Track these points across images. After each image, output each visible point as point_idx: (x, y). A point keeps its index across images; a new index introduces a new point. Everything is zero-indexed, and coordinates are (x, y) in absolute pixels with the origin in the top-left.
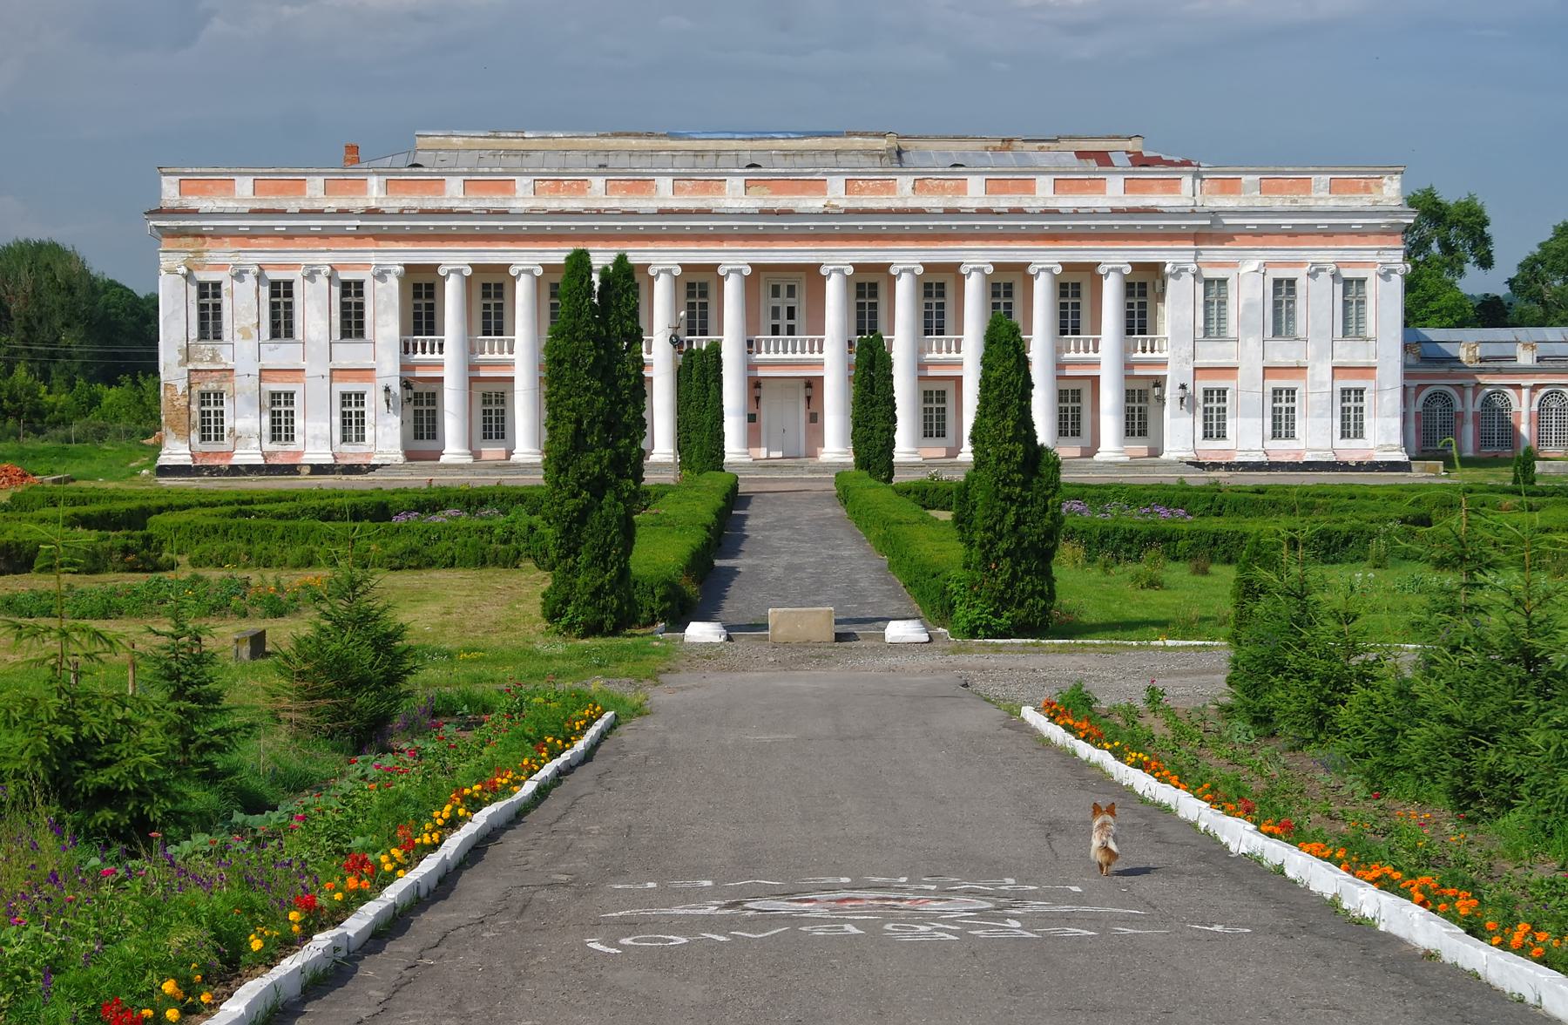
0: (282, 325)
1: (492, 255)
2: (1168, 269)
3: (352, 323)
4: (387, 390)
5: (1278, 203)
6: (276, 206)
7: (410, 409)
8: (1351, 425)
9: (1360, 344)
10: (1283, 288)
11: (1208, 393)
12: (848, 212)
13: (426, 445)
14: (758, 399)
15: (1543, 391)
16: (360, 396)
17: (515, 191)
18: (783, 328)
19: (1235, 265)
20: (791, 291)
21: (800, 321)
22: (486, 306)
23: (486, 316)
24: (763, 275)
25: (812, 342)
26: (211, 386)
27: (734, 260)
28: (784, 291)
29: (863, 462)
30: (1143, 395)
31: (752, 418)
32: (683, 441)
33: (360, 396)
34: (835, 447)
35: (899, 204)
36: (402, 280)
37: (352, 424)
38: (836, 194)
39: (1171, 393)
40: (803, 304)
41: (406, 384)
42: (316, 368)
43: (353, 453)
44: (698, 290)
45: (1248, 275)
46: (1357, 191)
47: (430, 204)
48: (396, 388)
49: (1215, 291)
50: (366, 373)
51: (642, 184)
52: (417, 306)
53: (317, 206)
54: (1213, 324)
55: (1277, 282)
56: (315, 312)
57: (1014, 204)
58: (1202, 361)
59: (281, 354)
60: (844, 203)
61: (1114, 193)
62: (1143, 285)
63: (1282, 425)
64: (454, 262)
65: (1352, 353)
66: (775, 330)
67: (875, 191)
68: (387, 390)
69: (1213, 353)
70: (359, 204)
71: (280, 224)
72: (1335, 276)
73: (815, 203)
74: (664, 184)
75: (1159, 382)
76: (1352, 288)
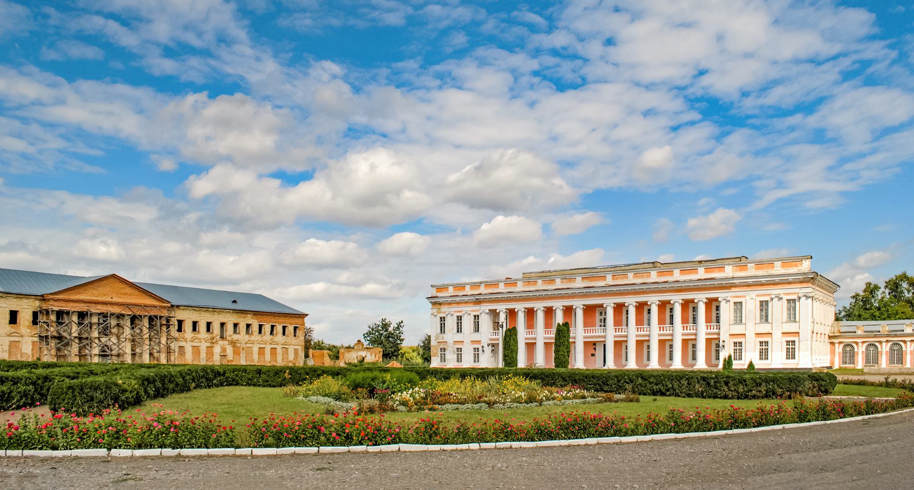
0: (459, 330)
2: (720, 299)
3: (477, 329)
5: (761, 273)
9: (793, 324)
10: (764, 305)
26: (442, 346)
27: (578, 304)
32: (505, 360)
37: (476, 358)
38: (609, 280)
43: (476, 365)
45: (751, 300)
48: (485, 346)
49: (738, 305)
50: (479, 342)
54: (739, 320)
55: (761, 302)
56: (468, 323)
59: (459, 337)
60: (611, 284)
69: (738, 329)
71: (458, 299)
73: (602, 283)
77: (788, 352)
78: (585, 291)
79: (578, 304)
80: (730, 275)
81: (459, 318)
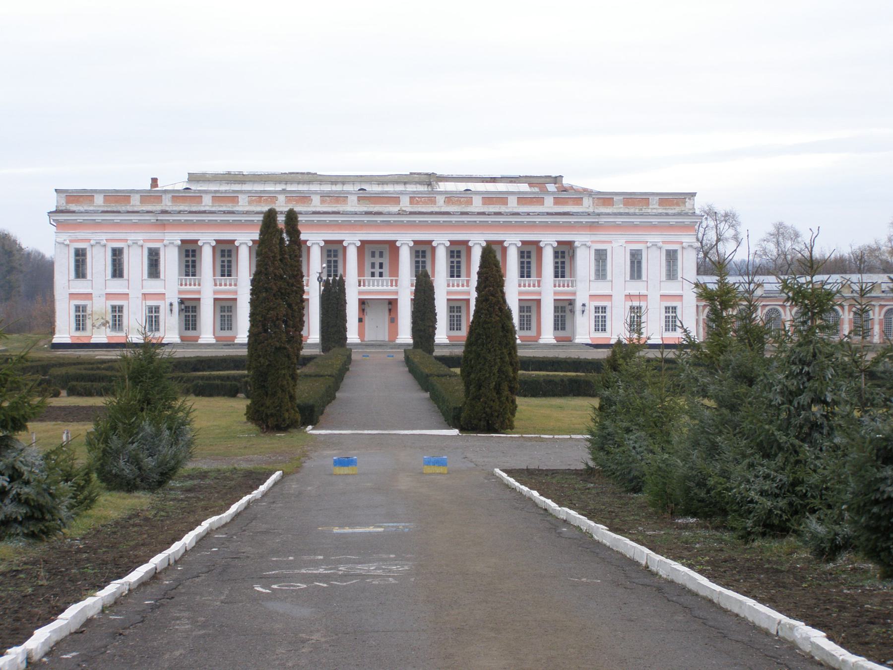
0: (117, 272)
1: (226, 235)
2: (576, 244)
3: (154, 269)
4: (171, 305)
6: (115, 209)
7: (183, 314)
11: (597, 308)
12: (411, 213)
13: (191, 333)
14: (363, 310)
15: (767, 308)
16: (157, 309)
17: (238, 202)
18: (377, 274)
19: (610, 242)
20: (381, 255)
21: (386, 270)
22: (223, 262)
23: (223, 266)
24: (366, 246)
25: (392, 281)
27: (352, 239)
28: (377, 254)
29: (416, 344)
30: (563, 309)
31: (360, 320)
33: (157, 309)
34: (405, 336)
35: (437, 210)
36: (180, 248)
39: (578, 307)
40: (388, 260)
41: (182, 301)
42: (135, 294)
44: (333, 252)
46: (673, 205)
47: (194, 209)
49: (601, 257)
52: (187, 261)
53: (136, 209)
54: (601, 273)
56: (135, 263)
57: (497, 210)
58: (593, 292)
59: (116, 286)
60: (409, 209)
61: (549, 204)
62: (563, 252)
64: (207, 239)
65: (672, 288)
66: (373, 275)
67: (425, 203)
68: (171, 305)
69: (601, 288)
70: (158, 208)
73: (395, 209)
74: (316, 199)
75: (571, 303)
76: (671, 257)
77: (667, 322)
78: (366, 219)
79: (352, 239)
80: (591, 210)
81: (117, 253)
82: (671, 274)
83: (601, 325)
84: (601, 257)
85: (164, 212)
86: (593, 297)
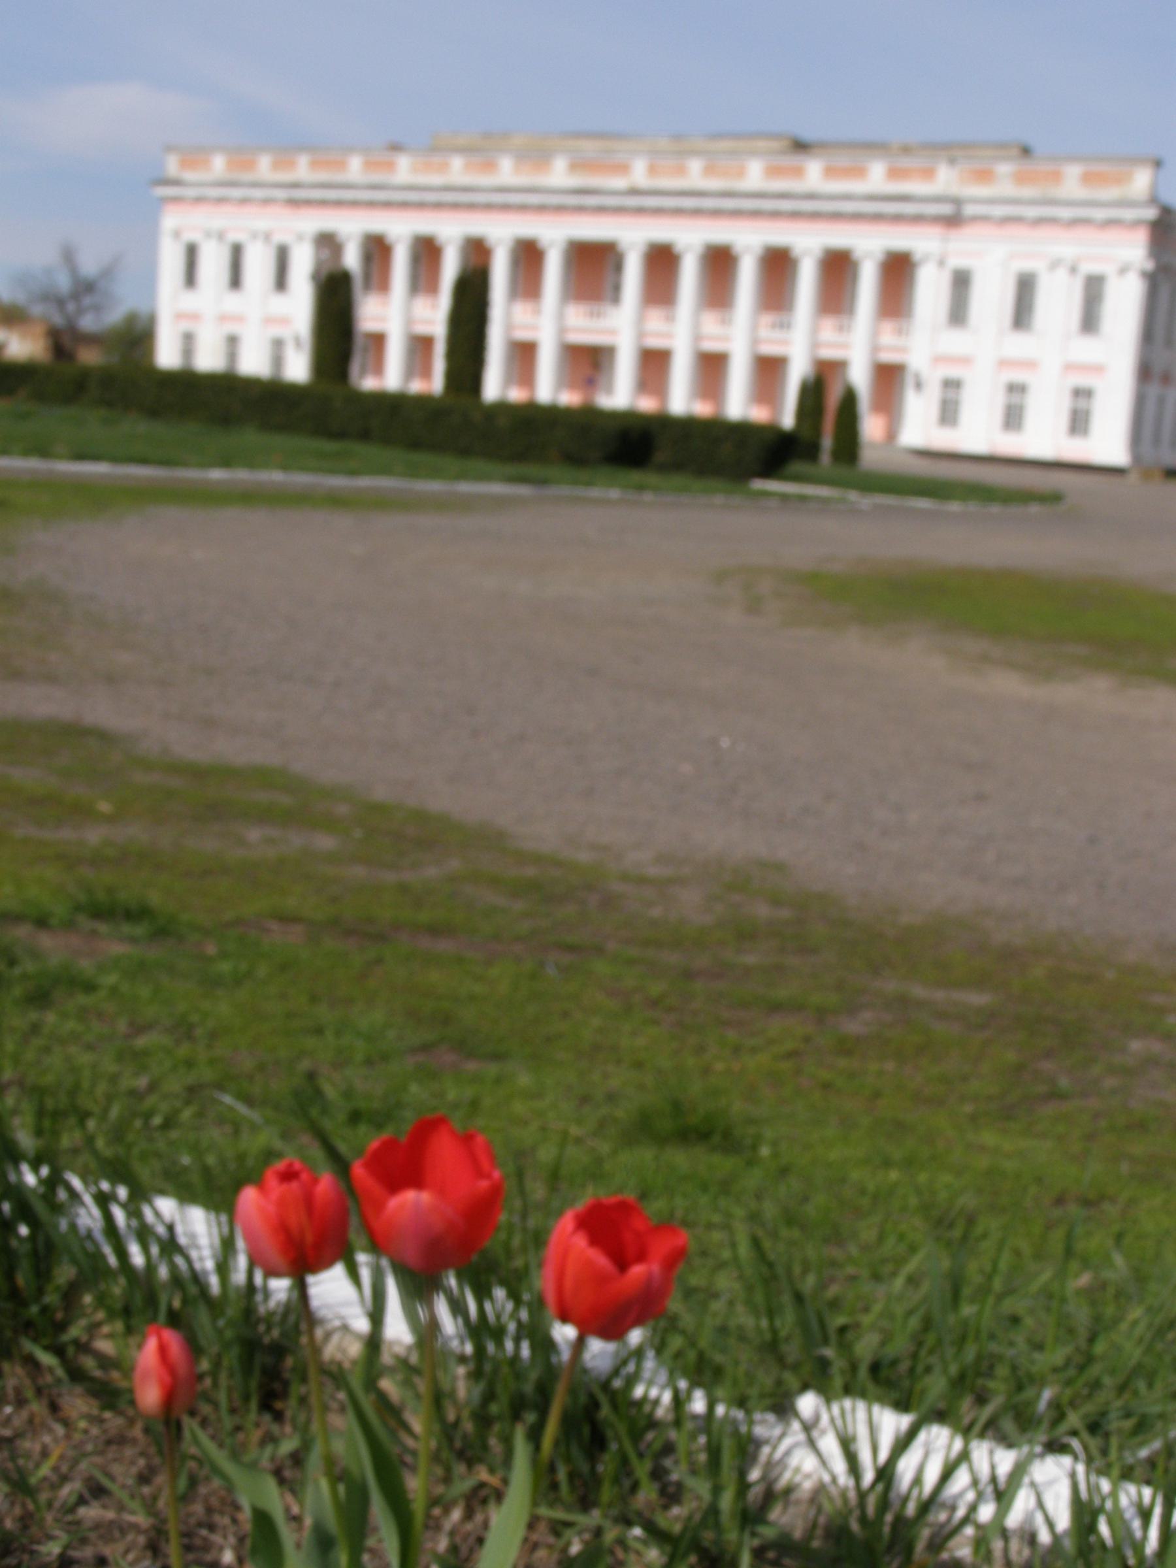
0: (236, 280)
8: (1079, 423)
49: (961, 281)
51: (490, 166)
54: (958, 314)
56: (259, 266)
63: (1013, 418)
72: (1073, 270)
82: (1090, 321)
83: (948, 413)
84: (961, 281)
85: (296, 185)
86: (939, 359)
